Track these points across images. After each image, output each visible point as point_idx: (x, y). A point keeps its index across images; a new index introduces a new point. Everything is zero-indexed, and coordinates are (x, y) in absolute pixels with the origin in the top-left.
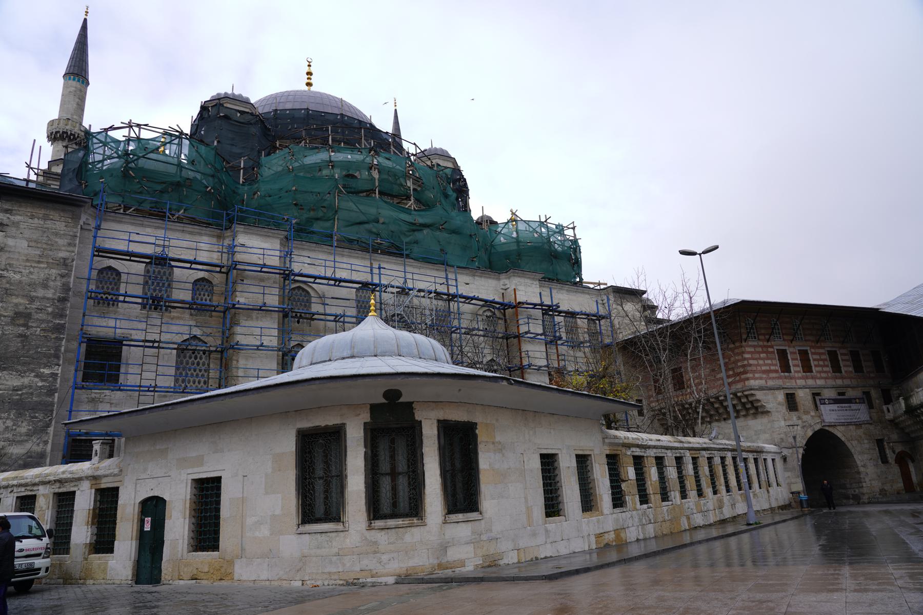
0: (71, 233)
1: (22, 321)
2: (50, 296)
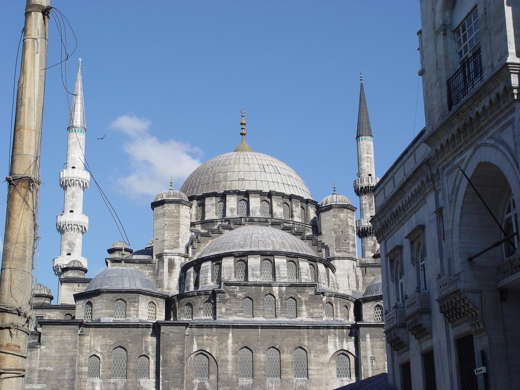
0: (74, 341)
2: (67, 378)
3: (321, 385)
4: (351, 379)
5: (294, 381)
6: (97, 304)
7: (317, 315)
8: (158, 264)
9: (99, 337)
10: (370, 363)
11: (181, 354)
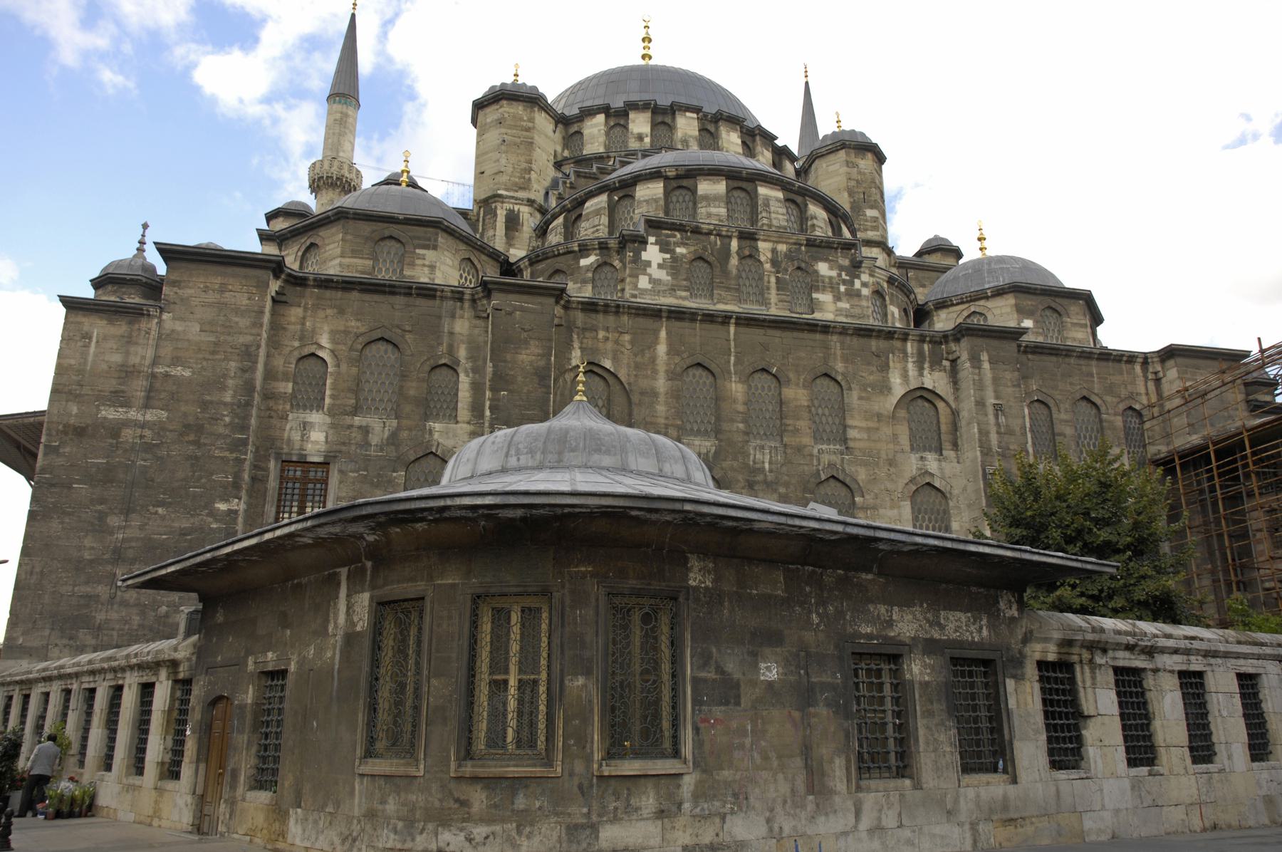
0: (256, 308)
1: (192, 437)
2: (228, 399)
3: (877, 464)
4: (941, 455)
5: (815, 451)
6: (332, 246)
7: (857, 311)
8: (484, 220)
9: (329, 311)
10: (991, 418)
11: (542, 363)
